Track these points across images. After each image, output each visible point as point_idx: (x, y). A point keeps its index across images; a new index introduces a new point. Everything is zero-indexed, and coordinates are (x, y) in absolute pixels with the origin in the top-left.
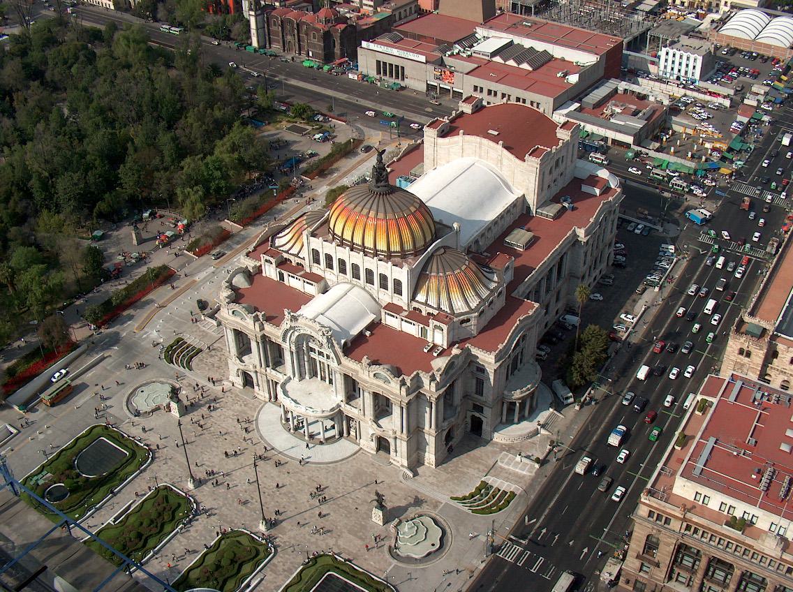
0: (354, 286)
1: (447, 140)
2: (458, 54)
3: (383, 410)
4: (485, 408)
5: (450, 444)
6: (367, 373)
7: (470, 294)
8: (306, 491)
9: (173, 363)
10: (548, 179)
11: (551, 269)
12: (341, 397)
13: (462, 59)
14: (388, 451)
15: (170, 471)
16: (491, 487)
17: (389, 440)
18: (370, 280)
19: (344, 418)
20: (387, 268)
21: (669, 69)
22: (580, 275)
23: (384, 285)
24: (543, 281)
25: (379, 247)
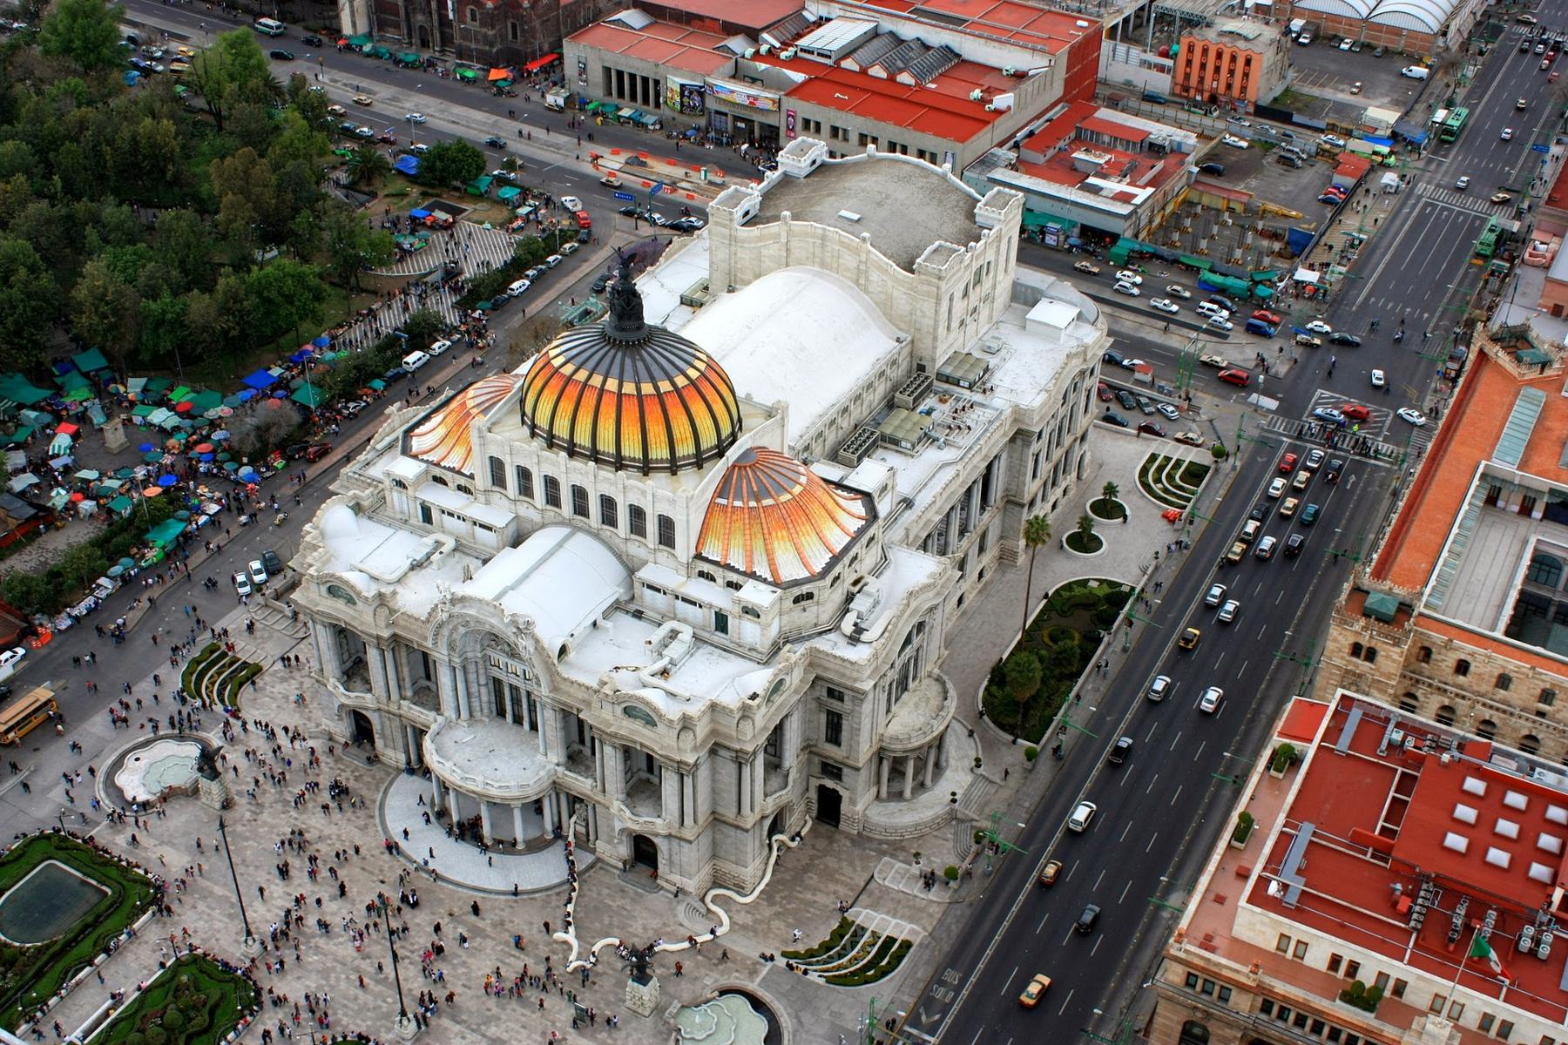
0: (577, 529)
1: (754, 231)
4: (846, 771)
6: (608, 707)
10: (959, 307)
11: (969, 491)
12: (556, 756)
15: (202, 923)
16: (864, 929)
17: (656, 840)
18: (609, 518)
21: (1194, 81)
22: (1027, 499)
24: (953, 514)
25: (626, 452)
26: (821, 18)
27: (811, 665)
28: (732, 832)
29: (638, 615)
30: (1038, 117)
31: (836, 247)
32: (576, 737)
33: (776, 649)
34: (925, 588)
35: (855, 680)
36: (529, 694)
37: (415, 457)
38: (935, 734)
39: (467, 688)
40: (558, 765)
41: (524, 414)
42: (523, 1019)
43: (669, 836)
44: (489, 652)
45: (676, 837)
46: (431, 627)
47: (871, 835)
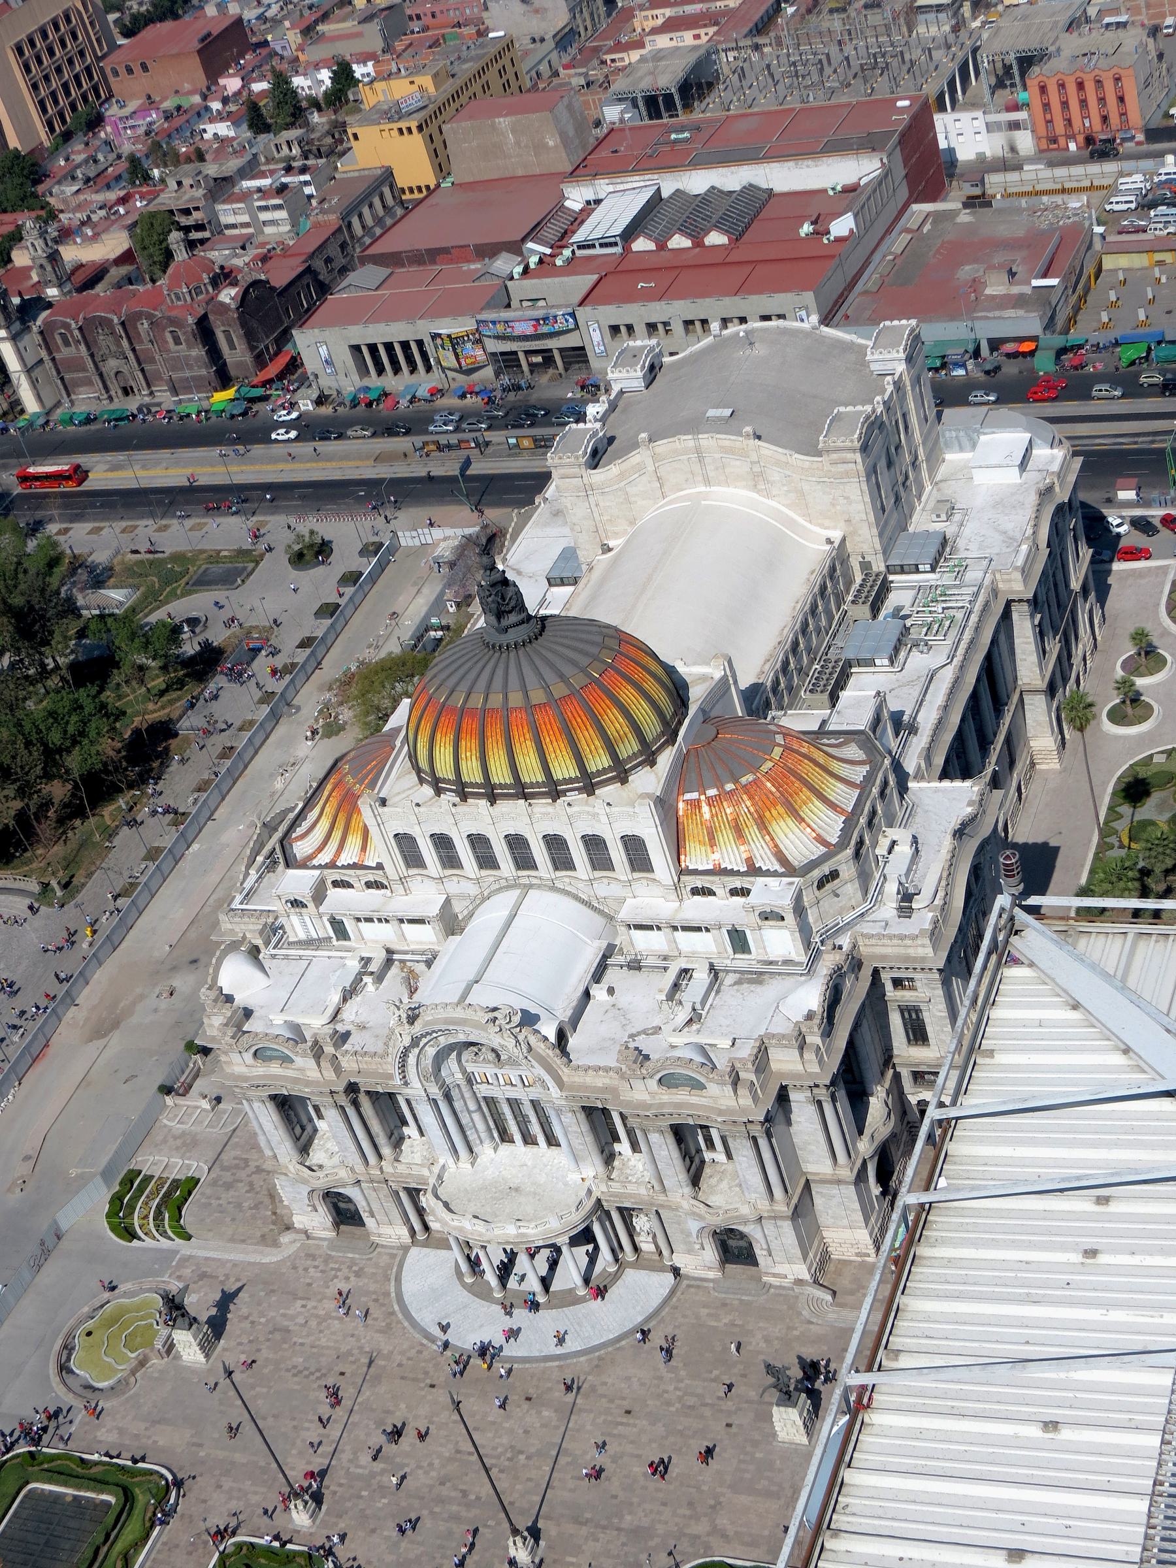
2: (541, 261)
6: (638, 1084)
7: (817, 812)
8: (589, 1427)
9: (139, 1239)
12: (592, 1167)
13: (556, 272)
15: (234, 1502)
19: (615, 1216)
20: (595, 816)
24: (966, 727)
25: (558, 775)
26: (588, 203)
29: (635, 965)
30: (888, 231)
31: (717, 456)
36: (535, 1104)
37: (303, 865)
41: (419, 771)
42: (661, 1495)
45: (770, 1218)
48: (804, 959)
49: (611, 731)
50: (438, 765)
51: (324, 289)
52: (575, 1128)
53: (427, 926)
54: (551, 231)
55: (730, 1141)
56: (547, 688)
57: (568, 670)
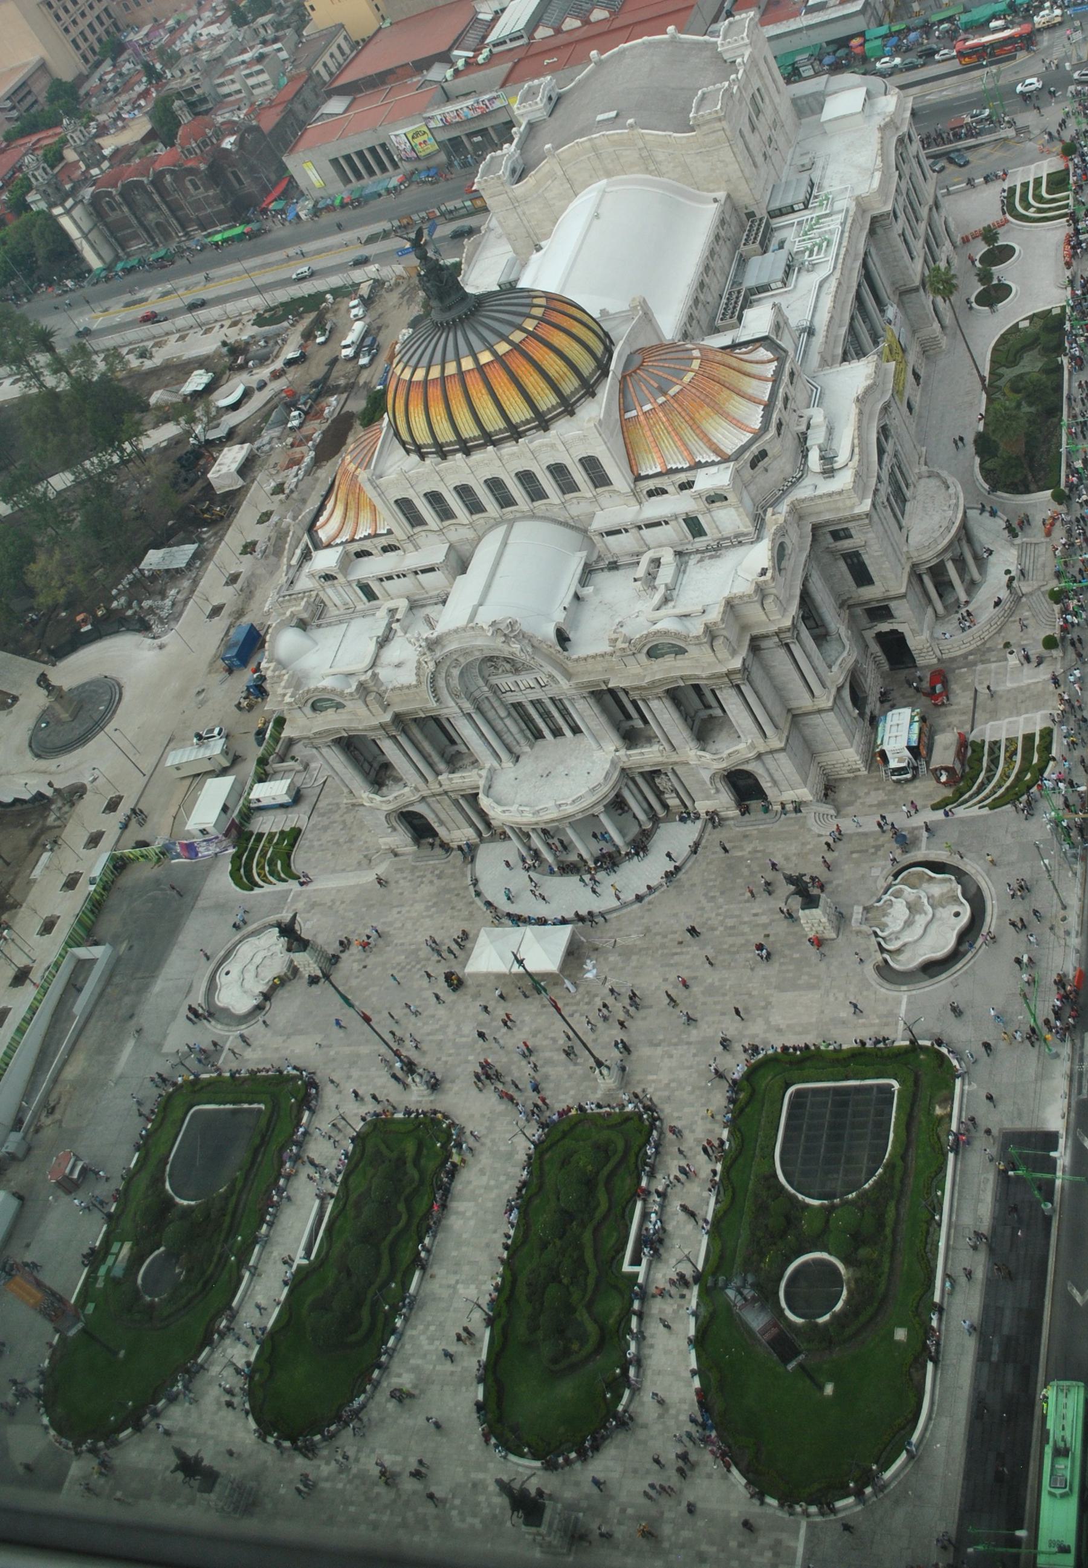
0: (511, 523)
1: (530, 181)
2: (468, 63)
3: (704, 721)
4: (893, 605)
5: (868, 711)
6: (631, 661)
7: (740, 408)
14: (760, 794)
18: (536, 493)
19: (640, 781)
23: (567, 486)
25: (516, 419)
26: (496, 12)
27: (801, 518)
28: (816, 719)
29: (614, 566)
32: (621, 717)
33: (759, 521)
34: (869, 390)
35: (852, 507)
37: (329, 546)
38: (957, 524)
39: (493, 728)
40: (617, 750)
41: (403, 443)
43: (759, 756)
44: (494, 680)
45: (767, 753)
46: (425, 688)
47: (953, 655)
48: (751, 529)
49: (552, 373)
50: (416, 434)
51: (302, 125)
52: (589, 712)
53: (438, 572)
54: (472, 39)
55: (718, 693)
56: (491, 349)
57: (504, 329)
